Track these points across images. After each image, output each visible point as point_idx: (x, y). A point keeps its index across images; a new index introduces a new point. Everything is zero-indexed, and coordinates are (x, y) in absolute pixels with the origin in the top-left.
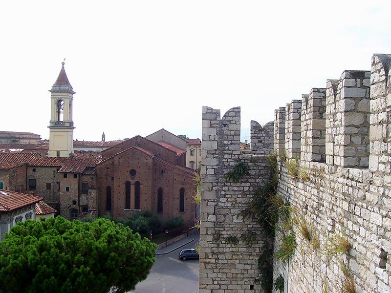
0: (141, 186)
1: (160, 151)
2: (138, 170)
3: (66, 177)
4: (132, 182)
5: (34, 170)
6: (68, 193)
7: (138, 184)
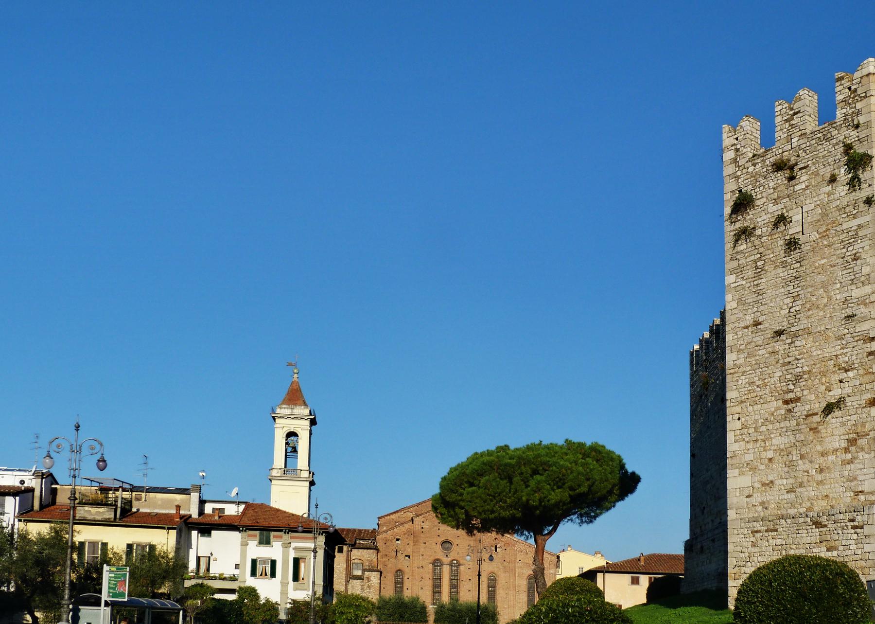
4: (446, 560)
7: (455, 566)
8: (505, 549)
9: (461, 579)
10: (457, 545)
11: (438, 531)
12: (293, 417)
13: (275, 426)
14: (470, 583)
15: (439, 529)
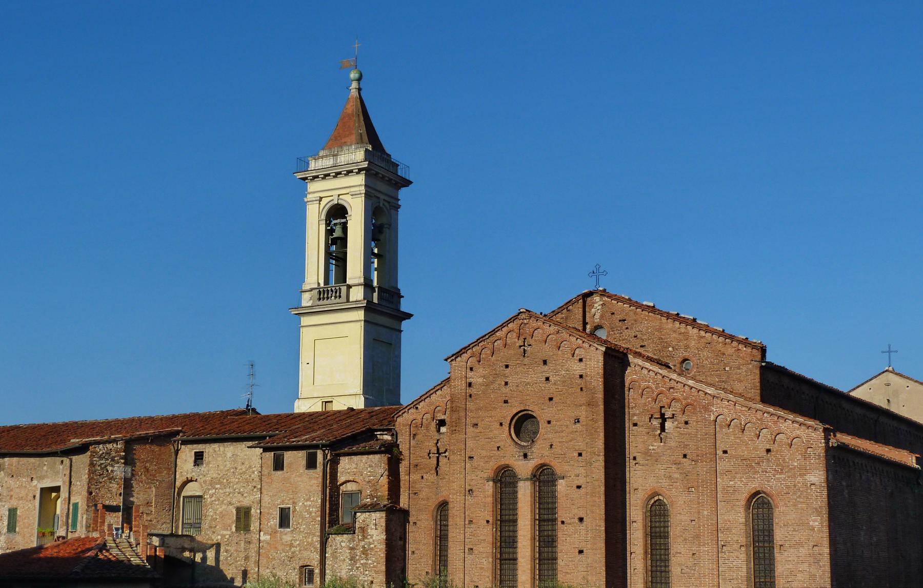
0: (561, 485)
1: (687, 347)
2: (542, 413)
3: (282, 469)
4: (524, 468)
5: (199, 457)
6: (287, 535)
8: (686, 423)
9: (560, 520)
10: (549, 422)
11: (505, 390)
12: (332, 172)
13: (306, 200)
14: (582, 527)
15: (506, 383)
